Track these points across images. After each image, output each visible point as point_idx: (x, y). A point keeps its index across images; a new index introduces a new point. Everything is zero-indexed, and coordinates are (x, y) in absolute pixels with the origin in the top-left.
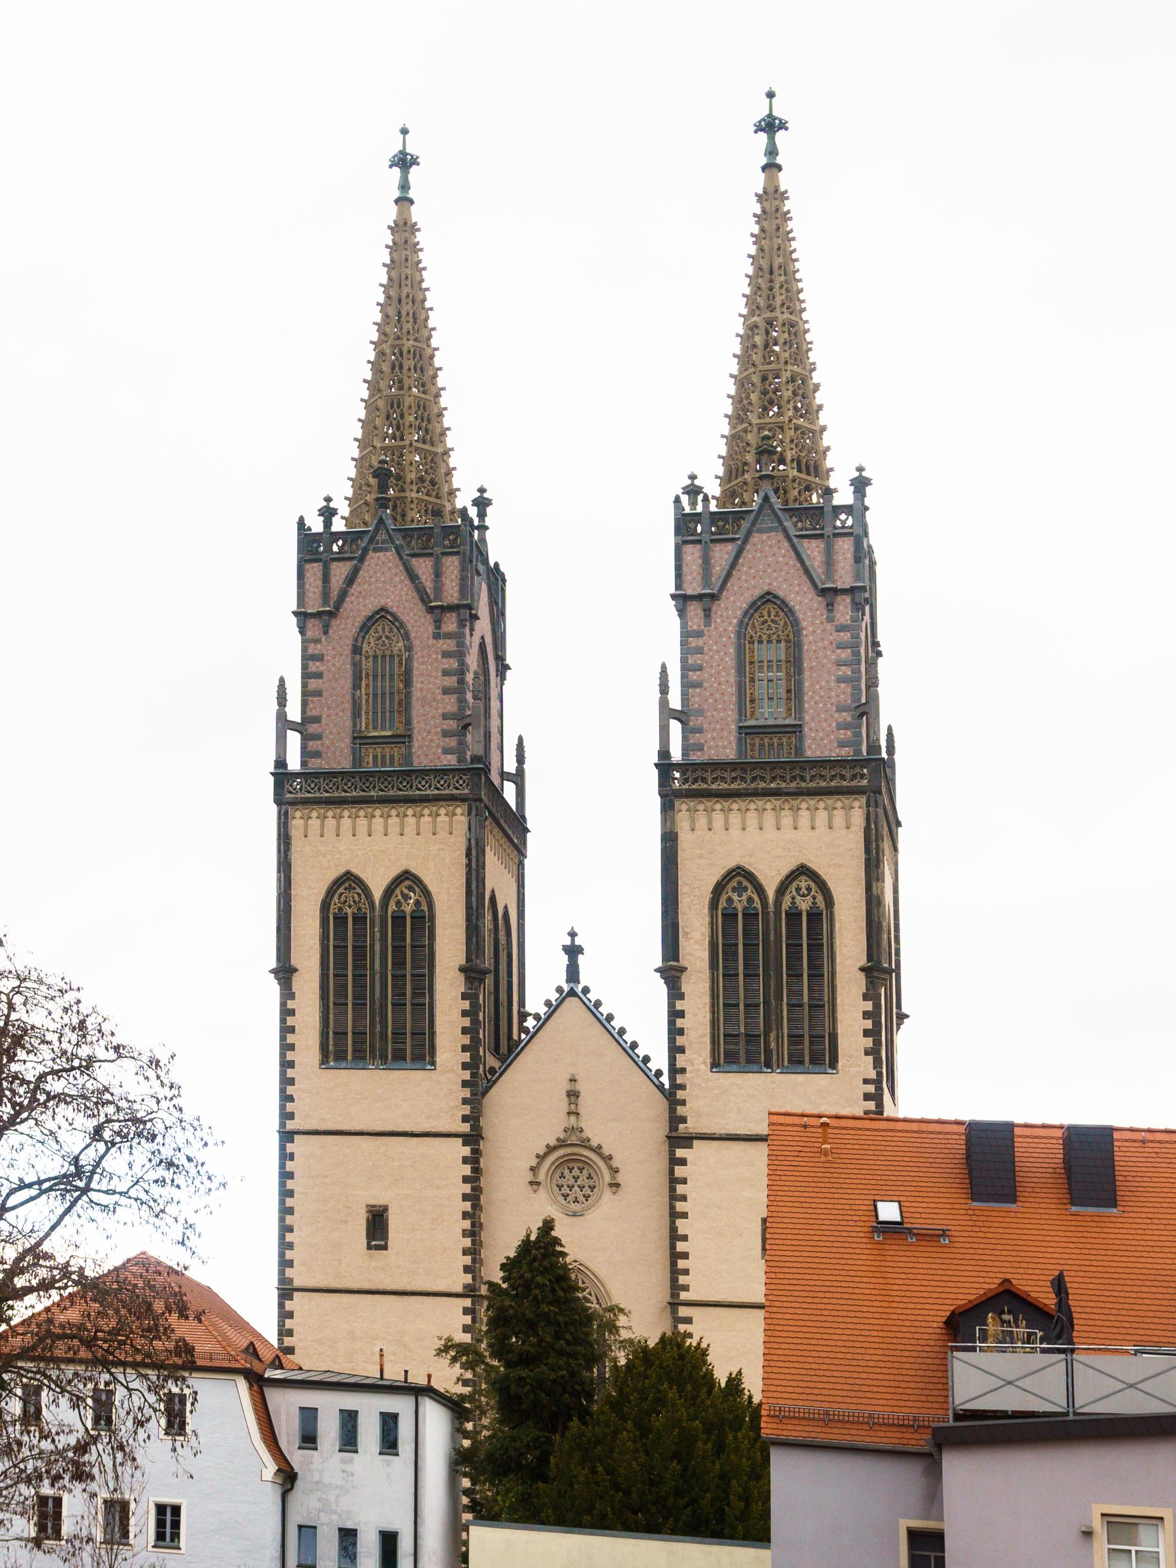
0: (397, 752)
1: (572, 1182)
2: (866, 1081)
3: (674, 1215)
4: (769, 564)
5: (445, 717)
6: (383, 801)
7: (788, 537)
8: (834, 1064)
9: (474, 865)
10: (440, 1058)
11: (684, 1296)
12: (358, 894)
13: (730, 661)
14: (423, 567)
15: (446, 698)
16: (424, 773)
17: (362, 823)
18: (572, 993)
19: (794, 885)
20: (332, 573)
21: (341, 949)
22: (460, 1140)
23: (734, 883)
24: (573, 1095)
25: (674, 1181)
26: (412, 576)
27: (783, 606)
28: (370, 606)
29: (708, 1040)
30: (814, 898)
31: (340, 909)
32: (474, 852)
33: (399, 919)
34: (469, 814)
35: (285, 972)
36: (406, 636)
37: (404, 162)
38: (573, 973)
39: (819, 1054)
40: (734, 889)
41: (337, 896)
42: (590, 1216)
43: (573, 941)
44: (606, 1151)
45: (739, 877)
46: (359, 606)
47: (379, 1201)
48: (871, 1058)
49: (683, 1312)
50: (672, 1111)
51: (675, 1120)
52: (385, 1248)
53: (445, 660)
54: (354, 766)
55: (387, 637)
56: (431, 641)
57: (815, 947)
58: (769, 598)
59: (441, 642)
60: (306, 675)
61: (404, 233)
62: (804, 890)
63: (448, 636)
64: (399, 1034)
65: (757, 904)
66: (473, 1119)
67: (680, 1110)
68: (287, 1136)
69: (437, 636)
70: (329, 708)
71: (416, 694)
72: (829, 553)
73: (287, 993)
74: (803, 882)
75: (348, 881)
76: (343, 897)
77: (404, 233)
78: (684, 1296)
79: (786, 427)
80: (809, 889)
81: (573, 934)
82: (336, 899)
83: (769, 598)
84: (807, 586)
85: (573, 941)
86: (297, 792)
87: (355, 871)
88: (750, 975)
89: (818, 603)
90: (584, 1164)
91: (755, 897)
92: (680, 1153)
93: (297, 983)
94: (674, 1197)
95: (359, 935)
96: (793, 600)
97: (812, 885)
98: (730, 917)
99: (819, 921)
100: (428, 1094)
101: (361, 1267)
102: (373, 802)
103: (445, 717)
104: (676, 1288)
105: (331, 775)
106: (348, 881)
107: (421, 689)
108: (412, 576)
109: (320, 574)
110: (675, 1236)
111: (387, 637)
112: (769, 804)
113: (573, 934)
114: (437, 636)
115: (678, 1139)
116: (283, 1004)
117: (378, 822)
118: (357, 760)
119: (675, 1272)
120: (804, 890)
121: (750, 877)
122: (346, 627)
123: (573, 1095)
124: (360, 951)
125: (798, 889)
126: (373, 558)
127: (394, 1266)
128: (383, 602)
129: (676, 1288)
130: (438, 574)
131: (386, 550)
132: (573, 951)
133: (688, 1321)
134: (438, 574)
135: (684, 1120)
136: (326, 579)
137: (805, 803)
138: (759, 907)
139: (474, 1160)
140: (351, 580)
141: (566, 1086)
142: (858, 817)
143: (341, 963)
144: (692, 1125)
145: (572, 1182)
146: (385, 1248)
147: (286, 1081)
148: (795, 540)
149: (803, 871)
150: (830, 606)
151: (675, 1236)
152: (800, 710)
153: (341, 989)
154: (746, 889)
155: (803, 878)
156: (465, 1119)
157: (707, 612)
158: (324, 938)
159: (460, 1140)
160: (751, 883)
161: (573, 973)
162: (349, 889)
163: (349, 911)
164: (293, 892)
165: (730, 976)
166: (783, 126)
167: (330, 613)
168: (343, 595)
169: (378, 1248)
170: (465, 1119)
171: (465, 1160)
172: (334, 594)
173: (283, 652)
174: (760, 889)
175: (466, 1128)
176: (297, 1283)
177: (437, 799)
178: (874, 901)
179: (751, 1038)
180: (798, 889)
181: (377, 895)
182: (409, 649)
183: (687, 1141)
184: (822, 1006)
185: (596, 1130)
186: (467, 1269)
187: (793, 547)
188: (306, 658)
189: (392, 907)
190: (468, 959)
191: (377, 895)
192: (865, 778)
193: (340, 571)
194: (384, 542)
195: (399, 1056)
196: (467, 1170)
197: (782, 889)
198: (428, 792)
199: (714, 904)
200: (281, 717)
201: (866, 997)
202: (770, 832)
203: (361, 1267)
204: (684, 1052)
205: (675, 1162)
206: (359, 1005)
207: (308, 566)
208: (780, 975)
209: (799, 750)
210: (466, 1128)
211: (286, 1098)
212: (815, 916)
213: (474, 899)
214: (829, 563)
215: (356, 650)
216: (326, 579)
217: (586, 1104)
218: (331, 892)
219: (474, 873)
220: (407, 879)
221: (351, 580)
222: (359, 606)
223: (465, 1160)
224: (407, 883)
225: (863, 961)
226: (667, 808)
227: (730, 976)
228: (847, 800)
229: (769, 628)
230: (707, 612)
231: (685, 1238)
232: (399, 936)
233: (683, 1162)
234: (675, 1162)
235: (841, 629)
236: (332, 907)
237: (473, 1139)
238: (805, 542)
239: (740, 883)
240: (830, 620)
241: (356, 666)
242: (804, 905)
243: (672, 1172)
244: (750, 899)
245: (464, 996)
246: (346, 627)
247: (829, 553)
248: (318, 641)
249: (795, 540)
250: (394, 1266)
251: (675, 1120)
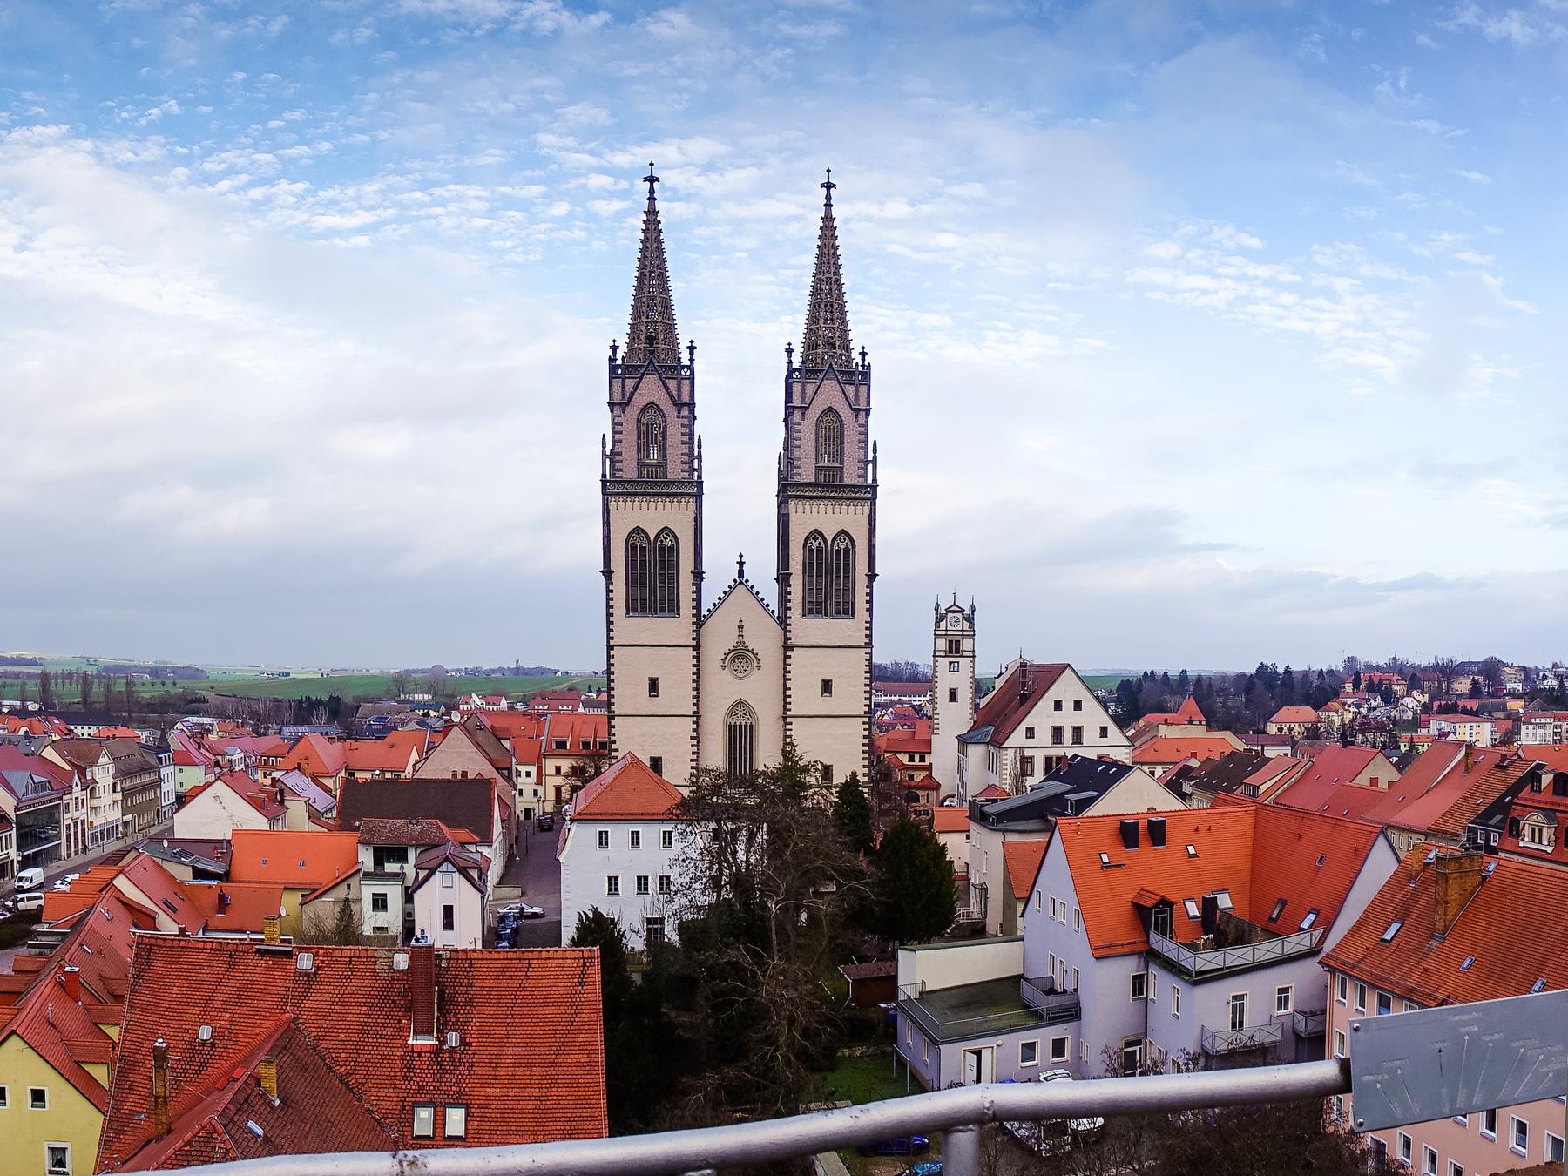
3: (786, 679)
4: (830, 394)
13: (813, 437)
14: (672, 384)
16: (674, 482)
17: (644, 504)
24: (741, 627)
25: (785, 665)
26: (667, 388)
33: (662, 548)
35: (608, 573)
39: (848, 610)
42: (748, 679)
46: (640, 400)
51: (787, 639)
58: (830, 410)
60: (614, 432)
64: (662, 601)
66: (697, 639)
68: (610, 648)
72: (857, 390)
73: (609, 582)
83: (830, 410)
86: (612, 487)
88: (819, 575)
90: (744, 657)
94: (786, 672)
96: (841, 411)
98: (811, 550)
99: (849, 552)
100: (677, 628)
104: (785, 710)
105: (628, 482)
106: (638, 530)
108: (667, 388)
110: (786, 688)
115: (787, 647)
118: (640, 475)
119: (785, 703)
122: (634, 410)
123: (741, 627)
124: (643, 562)
127: (661, 704)
129: (785, 710)
130: (679, 388)
132: (741, 564)
134: (679, 388)
136: (623, 387)
140: (635, 388)
142: (867, 510)
144: (793, 641)
149: (843, 532)
151: (786, 688)
152: (842, 461)
165: (811, 576)
168: (632, 395)
173: (603, 422)
179: (819, 603)
183: (791, 648)
184: (850, 590)
188: (614, 424)
193: (630, 384)
195: (662, 610)
200: (604, 452)
202: (837, 515)
203: (644, 702)
206: (643, 587)
209: (841, 479)
212: (847, 550)
214: (857, 396)
215: (639, 421)
216: (623, 387)
218: (629, 535)
220: (666, 530)
221: (635, 388)
222: (640, 400)
226: (783, 502)
227: (811, 576)
232: (662, 555)
234: (786, 657)
237: (697, 648)
241: (639, 429)
246: (634, 410)
247: (857, 390)
250: (661, 704)
251: (787, 639)
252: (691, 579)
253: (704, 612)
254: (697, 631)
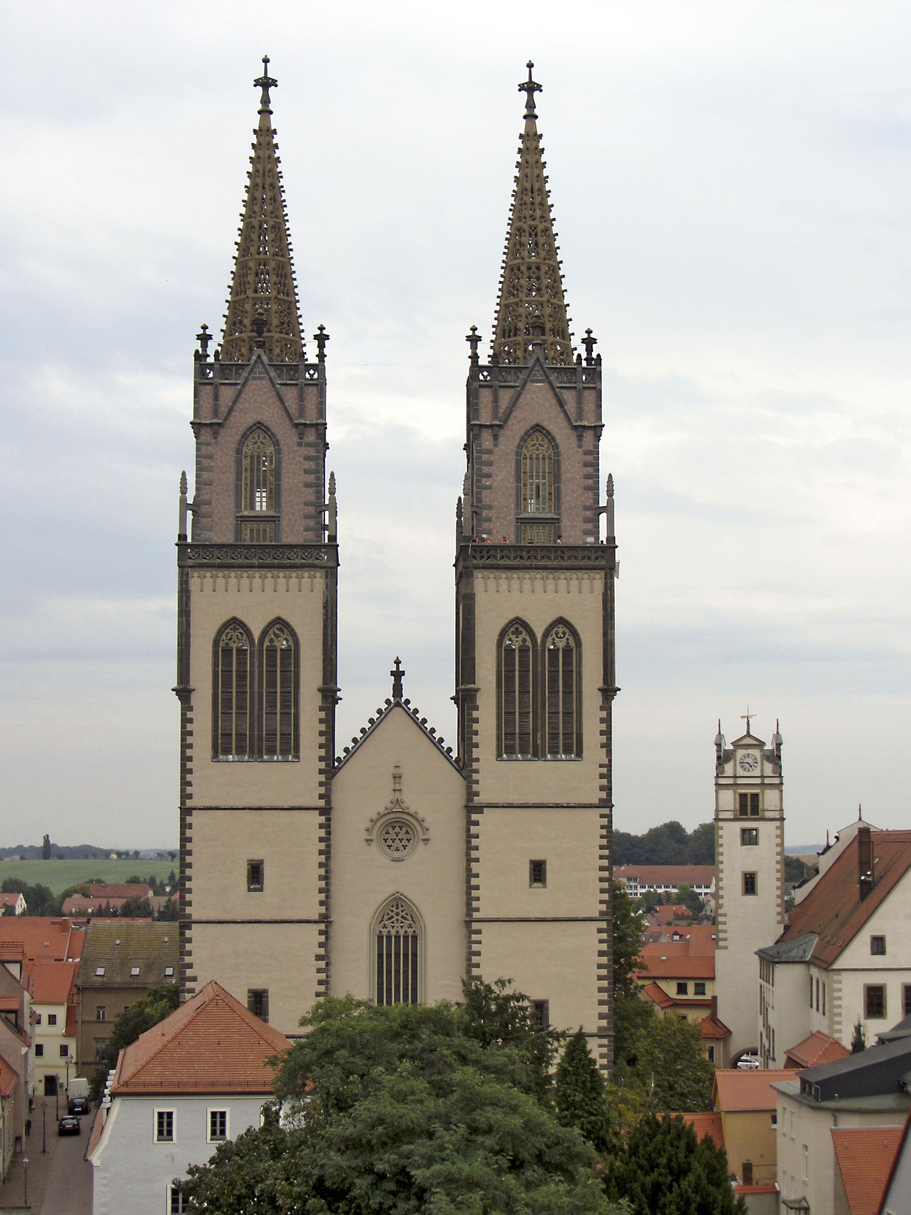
0: (269, 527)
1: (400, 836)
2: (601, 766)
5: (307, 504)
6: (261, 566)
7: (553, 388)
8: (579, 754)
9: (329, 614)
10: (303, 752)
11: (476, 915)
12: (242, 634)
15: (307, 490)
16: (291, 547)
18: (398, 704)
19: (555, 630)
20: (221, 394)
21: (227, 673)
22: (317, 812)
23: (513, 629)
24: (397, 777)
25: (469, 836)
27: (548, 435)
28: (249, 419)
29: (494, 738)
30: (568, 639)
31: (227, 644)
32: (329, 605)
34: (326, 577)
36: (276, 443)
37: (266, 83)
40: (513, 633)
41: (224, 635)
43: (398, 667)
44: (420, 816)
45: (518, 625)
46: (242, 419)
47: (257, 857)
48: (605, 749)
49: (475, 926)
50: (469, 788)
51: (471, 794)
52: (261, 890)
53: (306, 462)
54: (237, 540)
55: (262, 443)
56: (296, 448)
57: (568, 673)
59: (303, 448)
61: (265, 138)
62: (560, 635)
63: (308, 445)
65: (529, 643)
66: (326, 797)
67: (475, 787)
69: (300, 445)
70: (218, 494)
74: (561, 629)
75: (234, 623)
76: (229, 636)
77: (265, 138)
78: (476, 915)
79: (545, 304)
80: (564, 633)
81: (398, 662)
82: (224, 637)
84: (566, 424)
85: (398, 667)
87: (239, 616)
89: (573, 435)
91: (528, 638)
92: (474, 817)
93: (195, 700)
94: (470, 848)
95: (241, 663)
97: (567, 631)
98: (510, 651)
101: (244, 903)
102: (255, 567)
103: (307, 504)
104: (470, 910)
107: (288, 483)
109: (211, 395)
111: (262, 443)
112: (538, 575)
113: (398, 662)
114: (300, 445)
115: (472, 808)
116: (183, 715)
117: (257, 581)
118: (238, 533)
119: (469, 899)
120: (560, 635)
122: (230, 436)
123: (397, 777)
125: (557, 633)
126: (252, 383)
128: (259, 418)
129: (470, 910)
131: (263, 379)
133: (479, 932)
135: (477, 794)
136: (216, 398)
137: (562, 575)
138: (531, 646)
139: (327, 826)
141: (391, 770)
143: (227, 684)
145: (400, 836)
146: (261, 890)
147: (185, 771)
148: (557, 390)
150: (580, 437)
153: (227, 702)
154: (521, 633)
155: (561, 626)
156: (321, 797)
157: (496, 437)
158: (215, 664)
159: (317, 812)
160: (525, 628)
162: (235, 629)
163: (234, 646)
164: (192, 632)
166: (539, 88)
167: (220, 425)
169: (255, 890)
170: (321, 797)
171: (321, 826)
172: (223, 410)
174: (531, 633)
175: (322, 803)
176: (195, 917)
177: (302, 566)
178: (609, 644)
180: (557, 633)
181: (256, 635)
182: (278, 452)
183: (479, 809)
185: (414, 802)
186: (322, 903)
187: (556, 395)
189: (267, 643)
190: (324, 683)
191: (256, 635)
192: (602, 560)
194: (260, 373)
196: (322, 833)
197: (546, 634)
198: (296, 561)
199: (500, 643)
200: (183, 500)
201: (602, 709)
203: (244, 903)
204: (478, 747)
205: (471, 823)
206: (241, 714)
207: (202, 387)
208: (540, 692)
210: (322, 803)
211: (185, 783)
213: (329, 638)
215: (239, 451)
216: (216, 398)
217: (407, 783)
218: (220, 632)
219: (329, 621)
220: (279, 624)
222: (242, 419)
223: (321, 826)
224: (278, 626)
225: (600, 684)
228: (592, 574)
229: (537, 449)
230: (496, 437)
231: (477, 876)
233: (477, 823)
234: (471, 823)
236: (221, 642)
237: (325, 811)
238: (562, 391)
239: (517, 629)
240: (580, 446)
241: (239, 462)
242: (561, 644)
243: (468, 830)
244: (524, 640)
245: (321, 709)
246: (230, 436)
248: (208, 444)
249: (557, 390)
251: (471, 794)
252: (318, 699)
253: (339, 753)
254: (326, 784)
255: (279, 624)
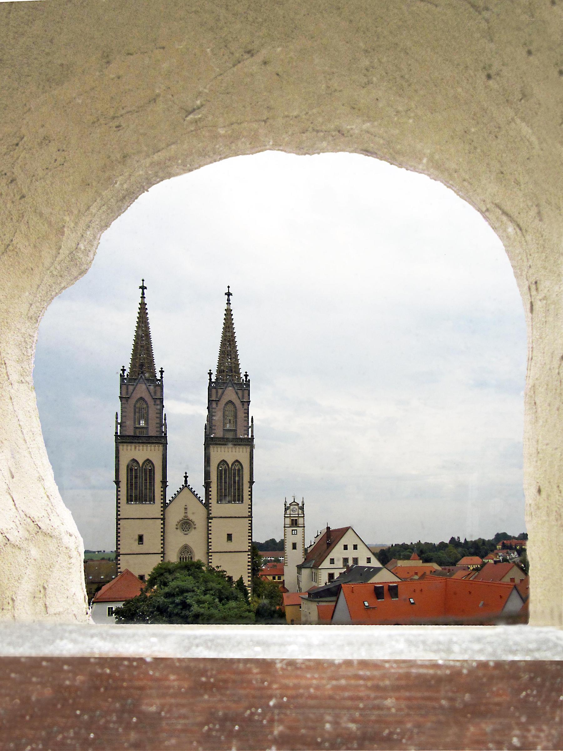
5: (157, 423)
8: (242, 502)
16: (152, 437)
21: (131, 476)
28: (139, 396)
36: (147, 404)
38: (186, 481)
45: (224, 462)
50: (208, 512)
71: (150, 417)
74: (237, 464)
94: (208, 530)
103: (157, 423)
118: (135, 432)
121: (226, 462)
136: (127, 389)
139: (163, 524)
141: (184, 507)
150: (243, 405)
157: (217, 404)
161: (186, 481)
174: (228, 465)
182: (148, 407)
185: (191, 517)
189: (144, 467)
199: (218, 468)
200: (117, 421)
203: (136, 547)
206: (136, 489)
208: (231, 484)
215: (135, 406)
220: (148, 461)
230: (217, 404)
235: (245, 410)
246: (132, 401)
251: (209, 514)
255: (148, 461)
